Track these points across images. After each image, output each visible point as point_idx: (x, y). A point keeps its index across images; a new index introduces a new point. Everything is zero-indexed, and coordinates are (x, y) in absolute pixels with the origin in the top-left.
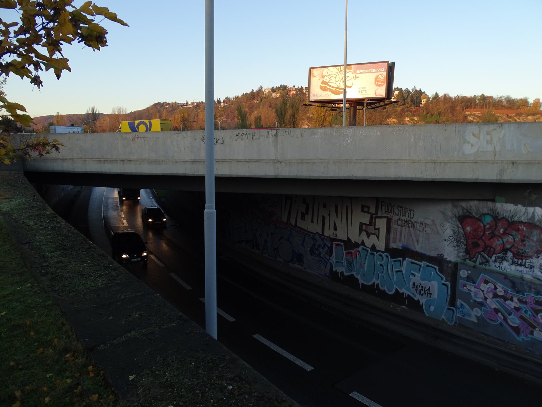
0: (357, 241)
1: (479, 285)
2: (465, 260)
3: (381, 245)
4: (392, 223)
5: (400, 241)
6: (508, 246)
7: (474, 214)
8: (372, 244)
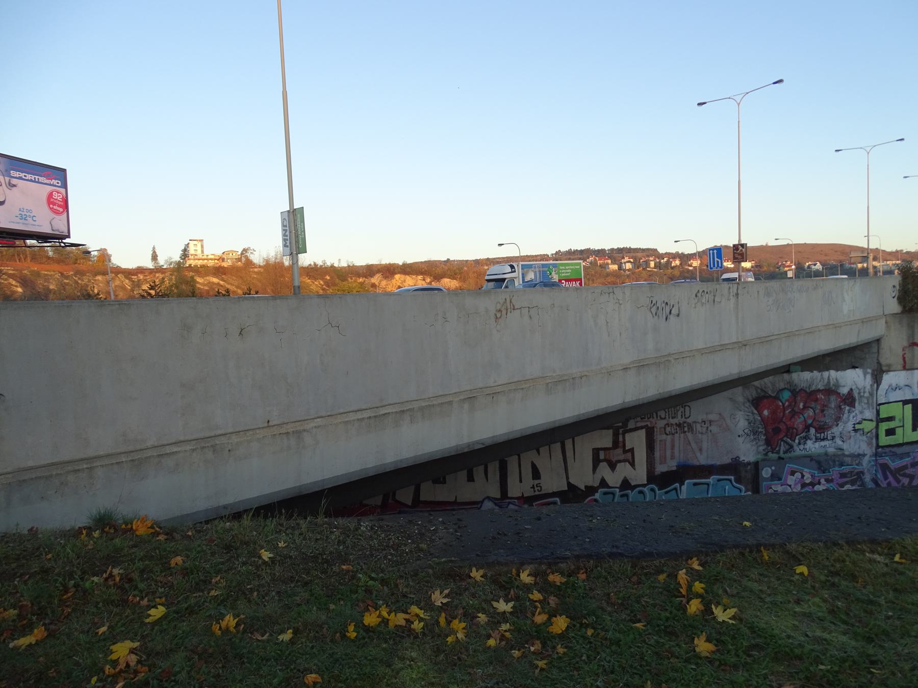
0: (590, 484)
1: (786, 480)
2: (766, 454)
3: (639, 475)
4: (655, 433)
5: (673, 457)
6: (810, 422)
7: (770, 392)
8: (622, 478)
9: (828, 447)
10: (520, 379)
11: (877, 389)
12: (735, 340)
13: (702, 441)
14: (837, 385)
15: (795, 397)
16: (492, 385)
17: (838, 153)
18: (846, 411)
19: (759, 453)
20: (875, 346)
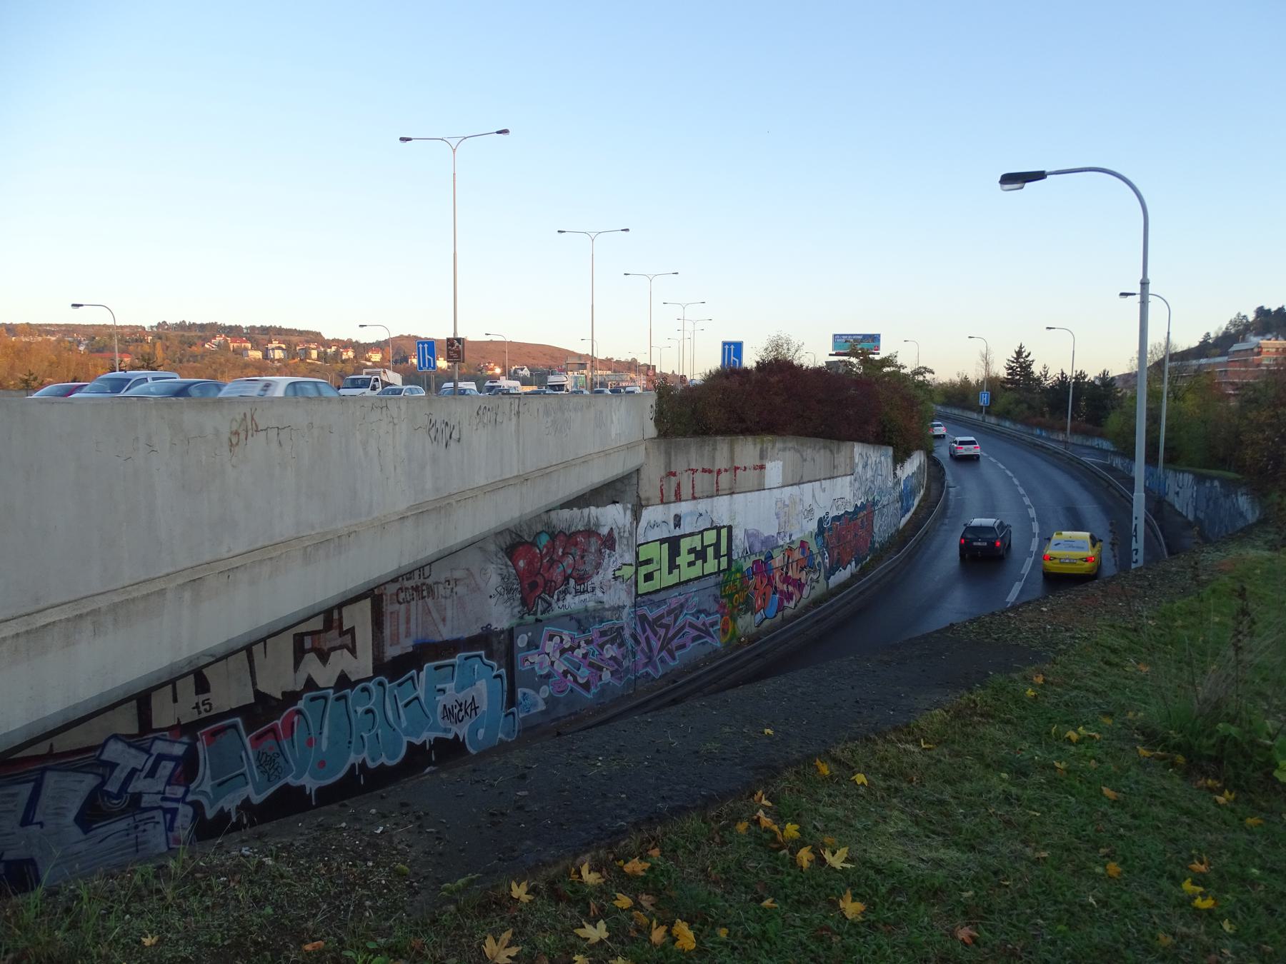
0: (290, 688)
1: (543, 648)
2: (522, 618)
3: (362, 665)
4: (384, 603)
5: (408, 634)
6: (569, 571)
7: (526, 538)
8: (337, 674)
9: (589, 601)
10: (266, 544)
11: (637, 527)
12: (516, 474)
13: (445, 609)
14: (598, 525)
15: (554, 541)
16: (226, 556)
17: (559, 234)
18: (607, 556)
19: (513, 616)
20: (635, 476)
